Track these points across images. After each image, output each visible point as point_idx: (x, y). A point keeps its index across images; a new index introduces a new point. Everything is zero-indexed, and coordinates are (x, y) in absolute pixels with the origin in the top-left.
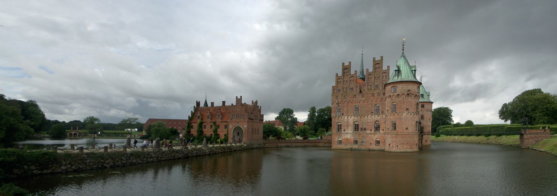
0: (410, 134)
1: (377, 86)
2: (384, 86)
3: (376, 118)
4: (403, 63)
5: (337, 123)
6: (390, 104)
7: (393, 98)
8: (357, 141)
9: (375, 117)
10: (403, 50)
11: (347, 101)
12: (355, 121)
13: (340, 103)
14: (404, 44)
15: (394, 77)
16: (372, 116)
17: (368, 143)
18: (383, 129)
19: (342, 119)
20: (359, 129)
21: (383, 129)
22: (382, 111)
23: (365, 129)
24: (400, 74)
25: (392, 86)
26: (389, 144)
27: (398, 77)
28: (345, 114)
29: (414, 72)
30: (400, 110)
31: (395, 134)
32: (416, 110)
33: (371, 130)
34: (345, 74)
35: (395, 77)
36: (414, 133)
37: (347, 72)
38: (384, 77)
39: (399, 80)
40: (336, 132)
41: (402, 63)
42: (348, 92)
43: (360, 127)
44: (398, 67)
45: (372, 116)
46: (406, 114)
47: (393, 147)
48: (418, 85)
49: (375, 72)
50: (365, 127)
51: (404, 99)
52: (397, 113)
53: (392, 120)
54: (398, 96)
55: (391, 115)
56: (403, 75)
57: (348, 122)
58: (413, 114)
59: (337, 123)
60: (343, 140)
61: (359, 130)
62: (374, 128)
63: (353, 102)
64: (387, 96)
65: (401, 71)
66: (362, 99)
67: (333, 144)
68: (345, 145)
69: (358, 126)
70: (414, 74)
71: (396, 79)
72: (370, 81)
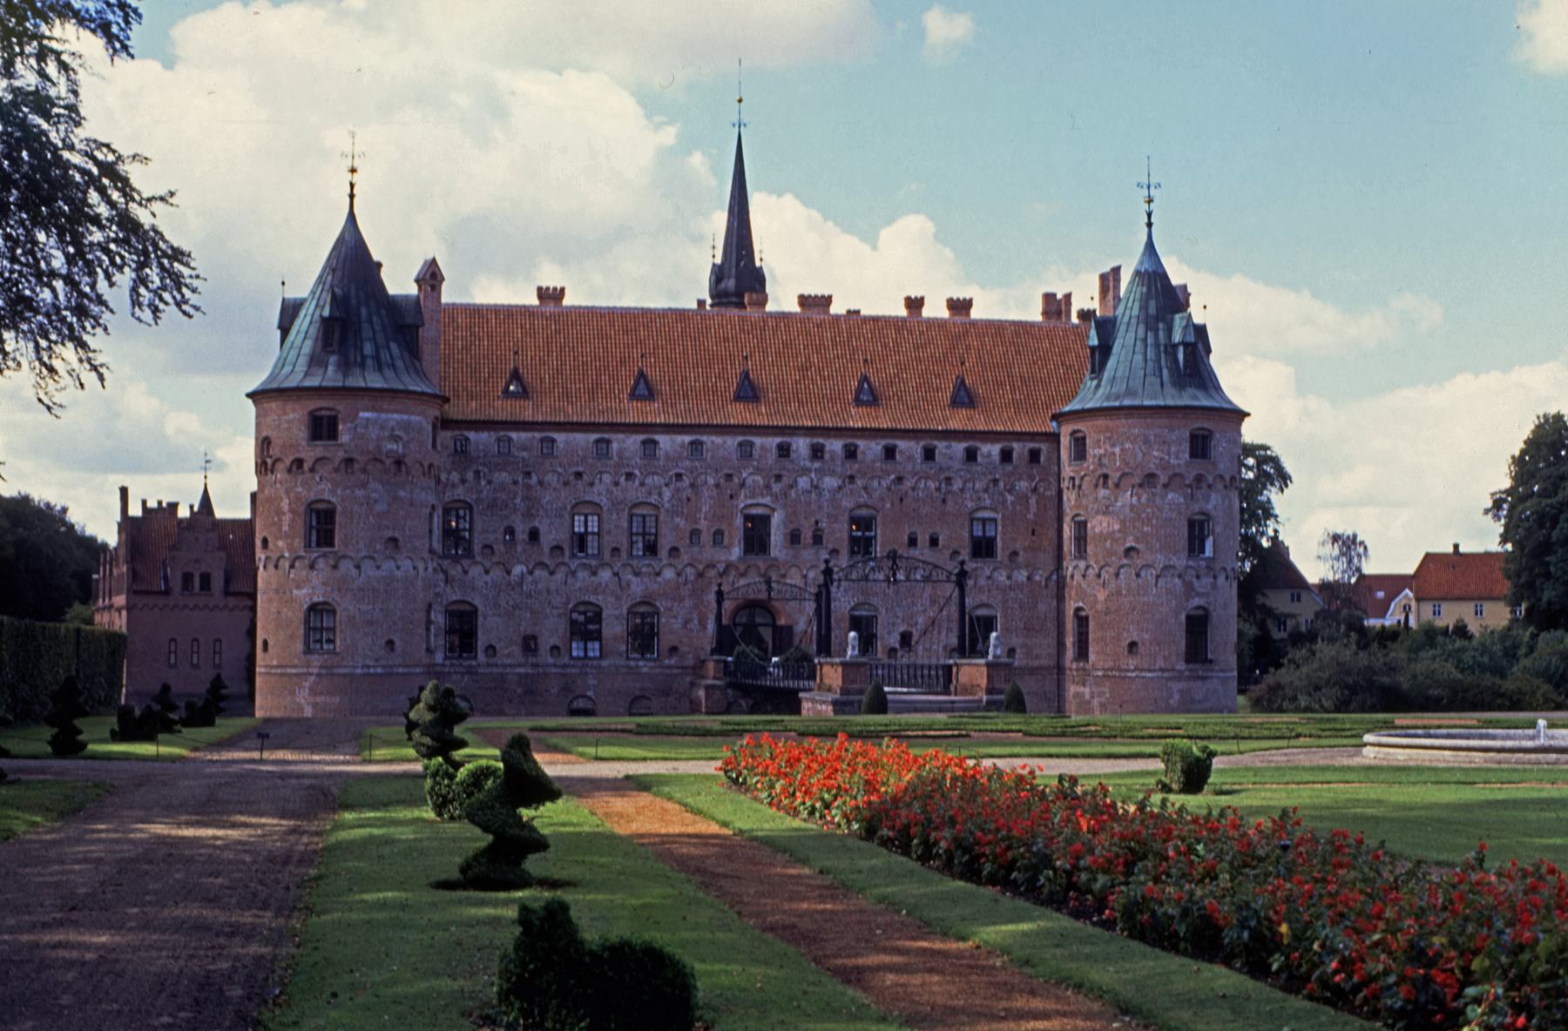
10: (352, 196)
36: (294, 671)
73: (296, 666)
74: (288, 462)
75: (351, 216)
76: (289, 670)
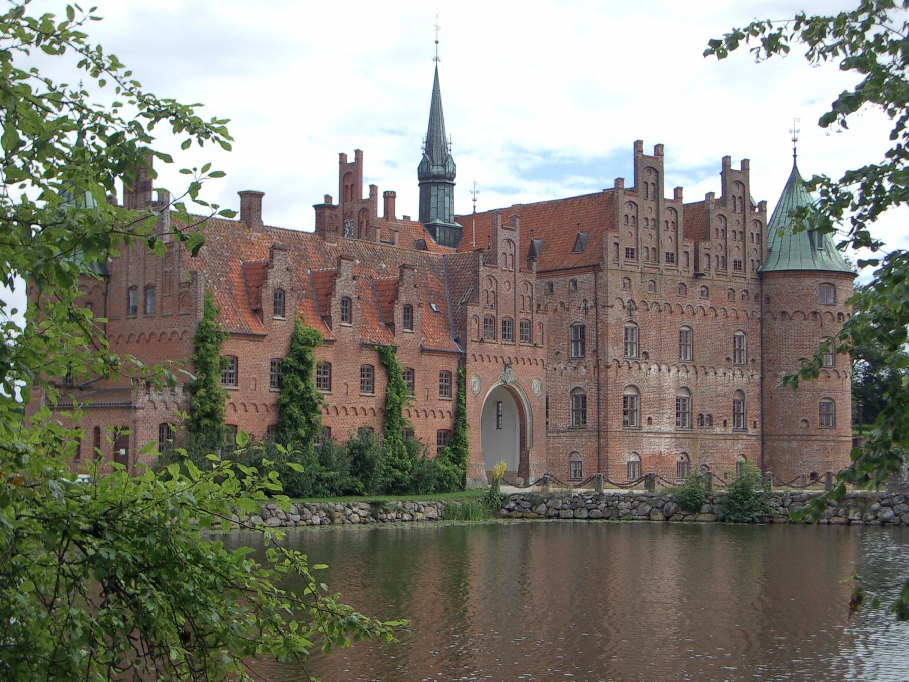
9: (734, 375)
10: (795, 156)
12: (683, 384)
14: (797, 136)
18: (755, 422)
25: (822, 280)
31: (834, 441)
33: (725, 422)
43: (698, 410)
52: (837, 371)
57: (660, 387)
60: (645, 459)
75: (795, 168)
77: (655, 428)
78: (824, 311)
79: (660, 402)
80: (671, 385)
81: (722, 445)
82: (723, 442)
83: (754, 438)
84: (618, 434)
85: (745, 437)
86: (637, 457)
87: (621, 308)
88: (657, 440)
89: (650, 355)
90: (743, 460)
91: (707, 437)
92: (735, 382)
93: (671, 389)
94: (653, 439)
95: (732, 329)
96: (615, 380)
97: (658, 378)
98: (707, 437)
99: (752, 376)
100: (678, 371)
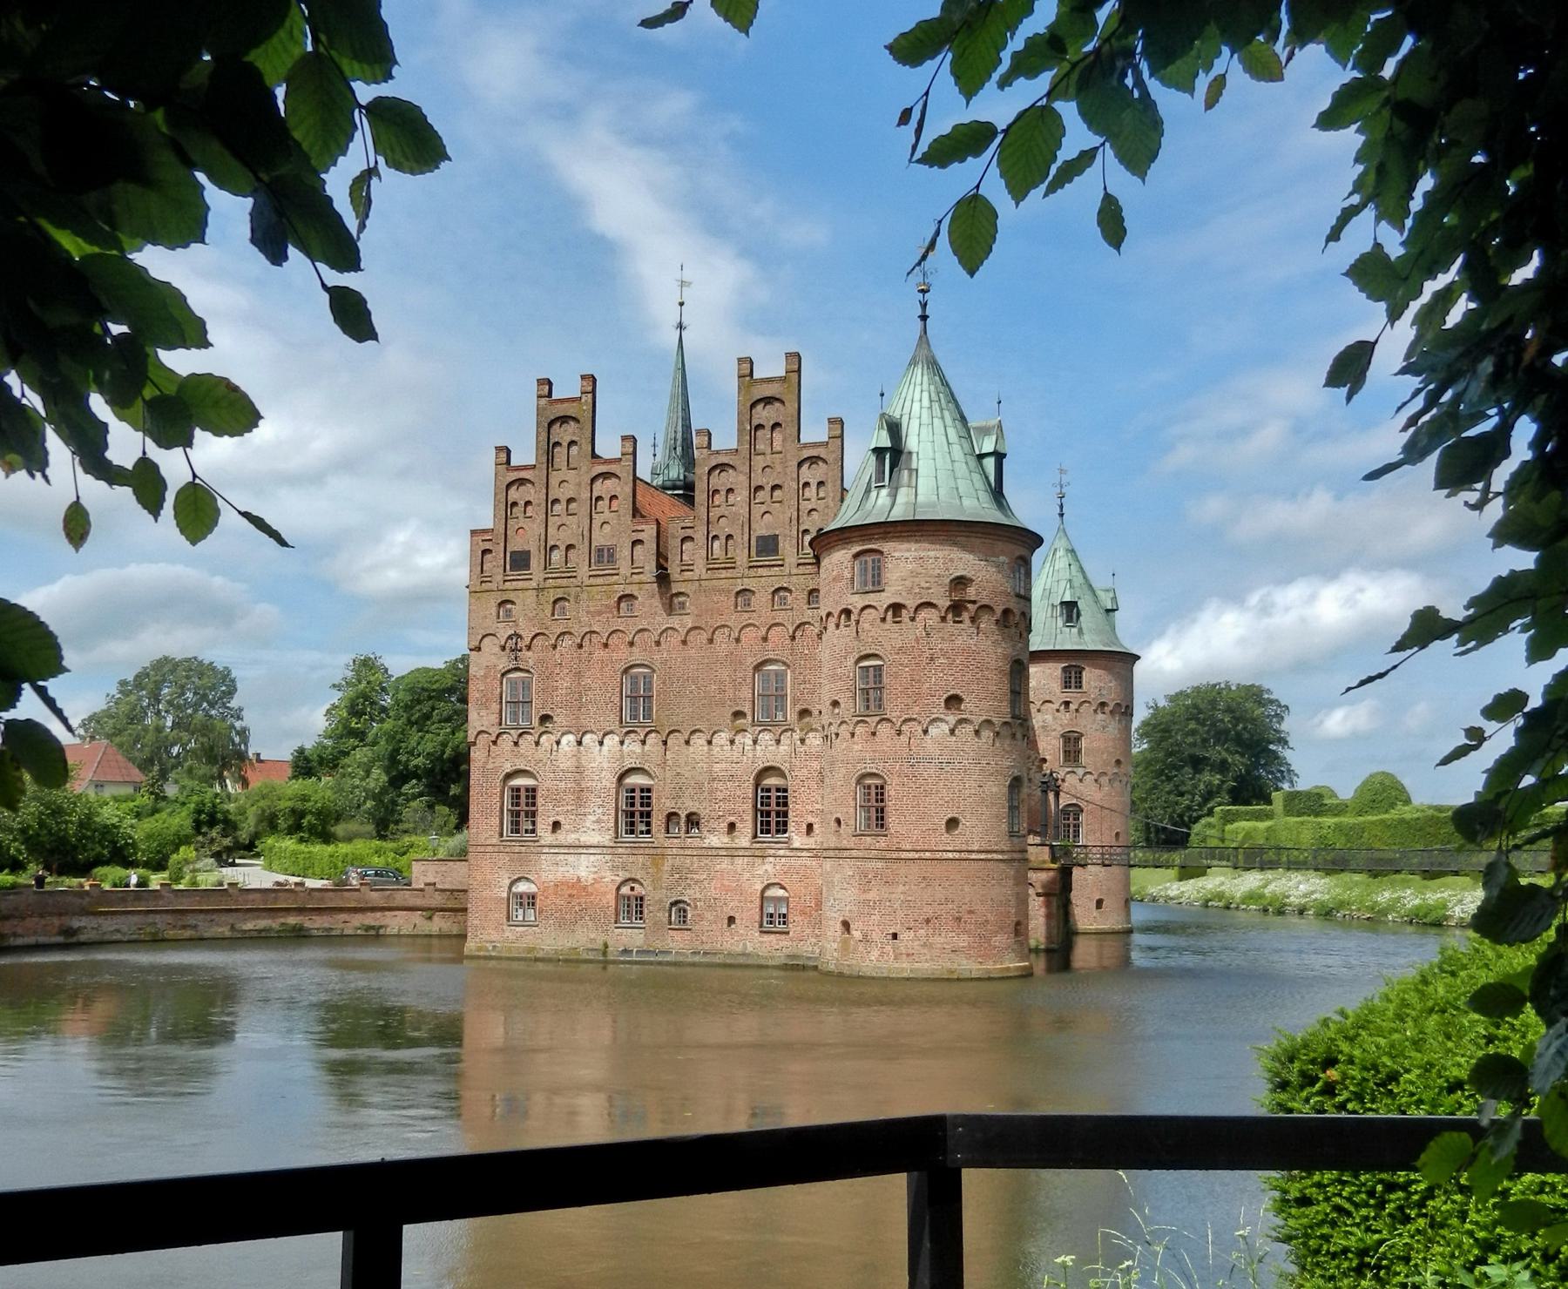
0: (974, 856)
1: (768, 545)
2: (811, 544)
3: (768, 750)
4: (926, 402)
5: (509, 776)
6: (851, 661)
7: (867, 626)
8: (642, 899)
9: (755, 742)
10: (924, 318)
11: (579, 631)
12: (628, 764)
13: (529, 648)
15: (868, 491)
16: (738, 738)
17: (709, 915)
18: (810, 827)
19: (541, 753)
20: (658, 820)
21: (810, 827)
22: (799, 707)
23: (693, 821)
24: (906, 473)
25: (857, 548)
26: (846, 925)
27: (894, 496)
28: (560, 719)
29: (990, 463)
30: (910, 701)
32: (1005, 708)
34: (560, 453)
35: (874, 494)
37: (572, 443)
38: (814, 487)
39: (898, 514)
40: (495, 841)
41: (916, 406)
42: (583, 571)
44: (894, 429)
45: (738, 738)
46: (945, 728)
47: (866, 939)
48: (1021, 551)
49: (753, 451)
50: (691, 806)
51: (935, 636)
52: (888, 720)
53: (862, 768)
54: (894, 616)
55: (853, 735)
56: (925, 485)
57: (579, 769)
58: (987, 734)
59: (509, 776)
61: (654, 830)
62: (749, 818)
63: (614, 640)
64: (829, 614)
65: (910, 453)
66: (674, 621)
67: (473, 919)
68: (561, 924)
69: (646, 801)
70: (992, 479)
71: (881, 506)
72: (723, 510)
73: (1002, 852)
74: (999, 610)
76: (995, 856)
77: (563, 837)
78: (860, 606)
79: (580, 795)
80: (605, 765)
81: (724, 866)
82: (726, 860)
83: (804, 854)
84: (490, 849)
85: (781, 852)
86: (533, 886)
87: (497, 649)
88: (571, 858)
89: (555, 719)
90: (781, 893)
91: (689, 852)
92: (759, 753)
93: (604, 773)
94: (561, 857)
95: (750, 660)
96: (486, 763)
97: (577, 756)
98: (689, 852)
99: (802, 741)
100: (622, 743)
